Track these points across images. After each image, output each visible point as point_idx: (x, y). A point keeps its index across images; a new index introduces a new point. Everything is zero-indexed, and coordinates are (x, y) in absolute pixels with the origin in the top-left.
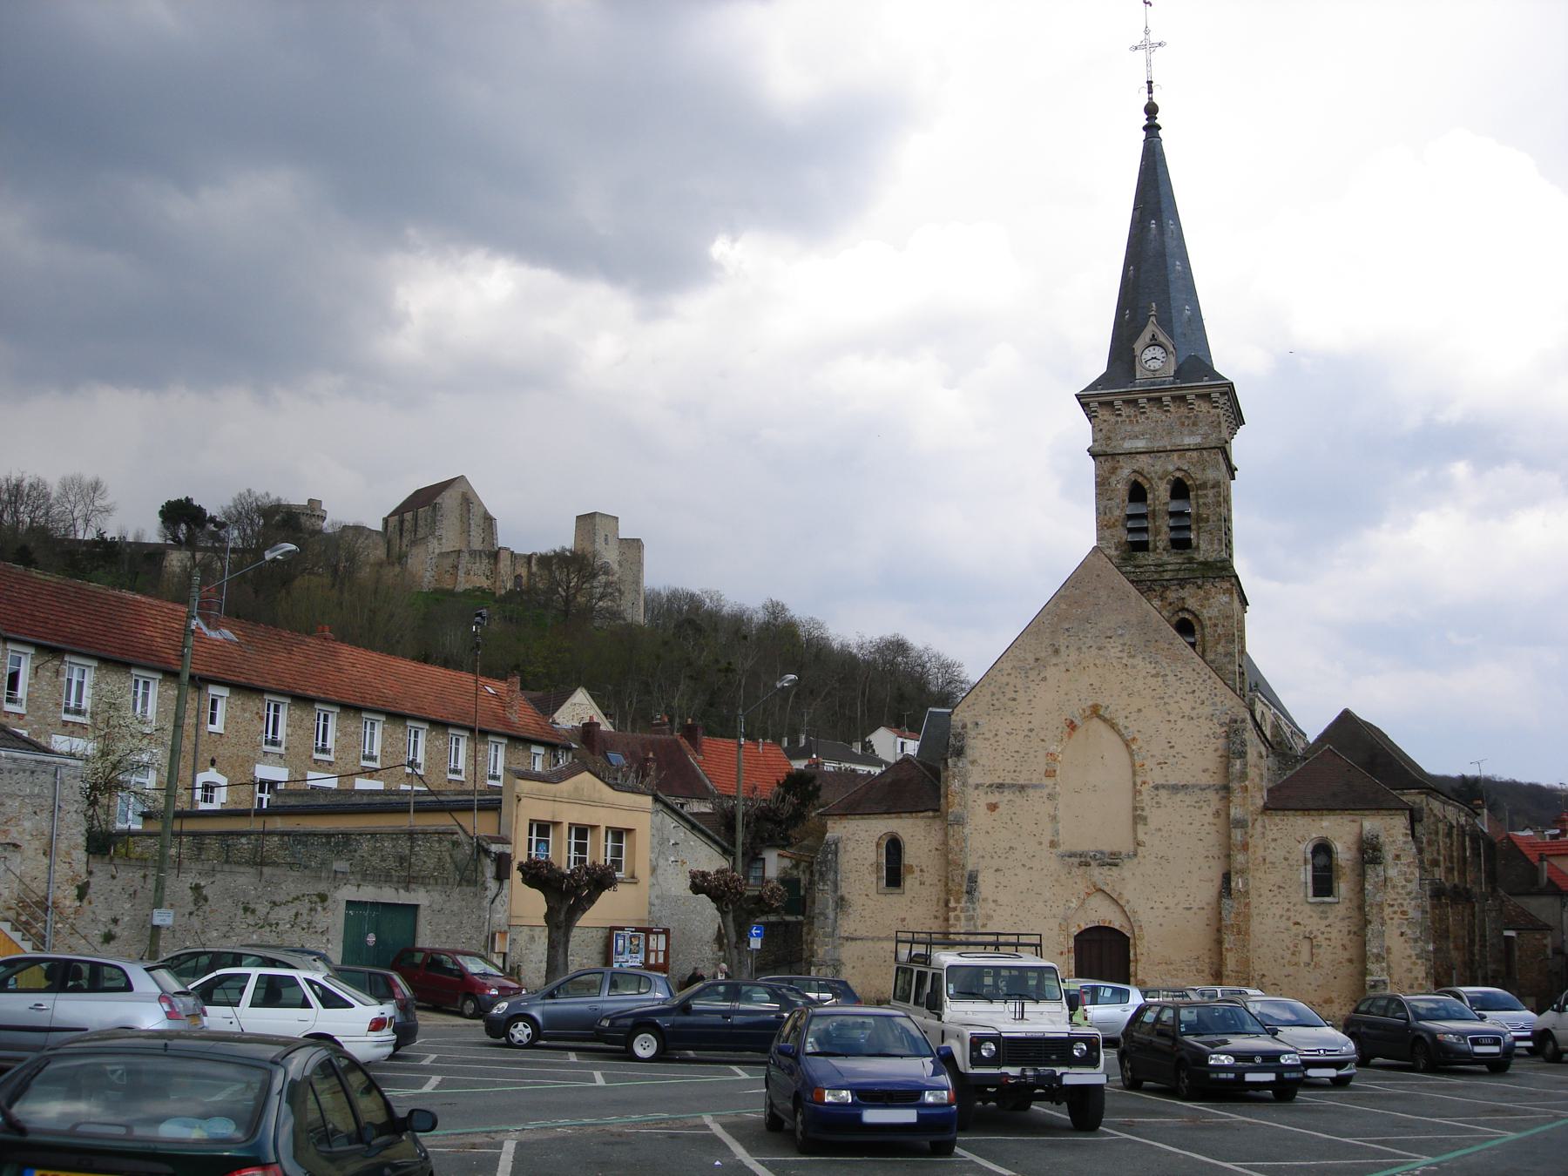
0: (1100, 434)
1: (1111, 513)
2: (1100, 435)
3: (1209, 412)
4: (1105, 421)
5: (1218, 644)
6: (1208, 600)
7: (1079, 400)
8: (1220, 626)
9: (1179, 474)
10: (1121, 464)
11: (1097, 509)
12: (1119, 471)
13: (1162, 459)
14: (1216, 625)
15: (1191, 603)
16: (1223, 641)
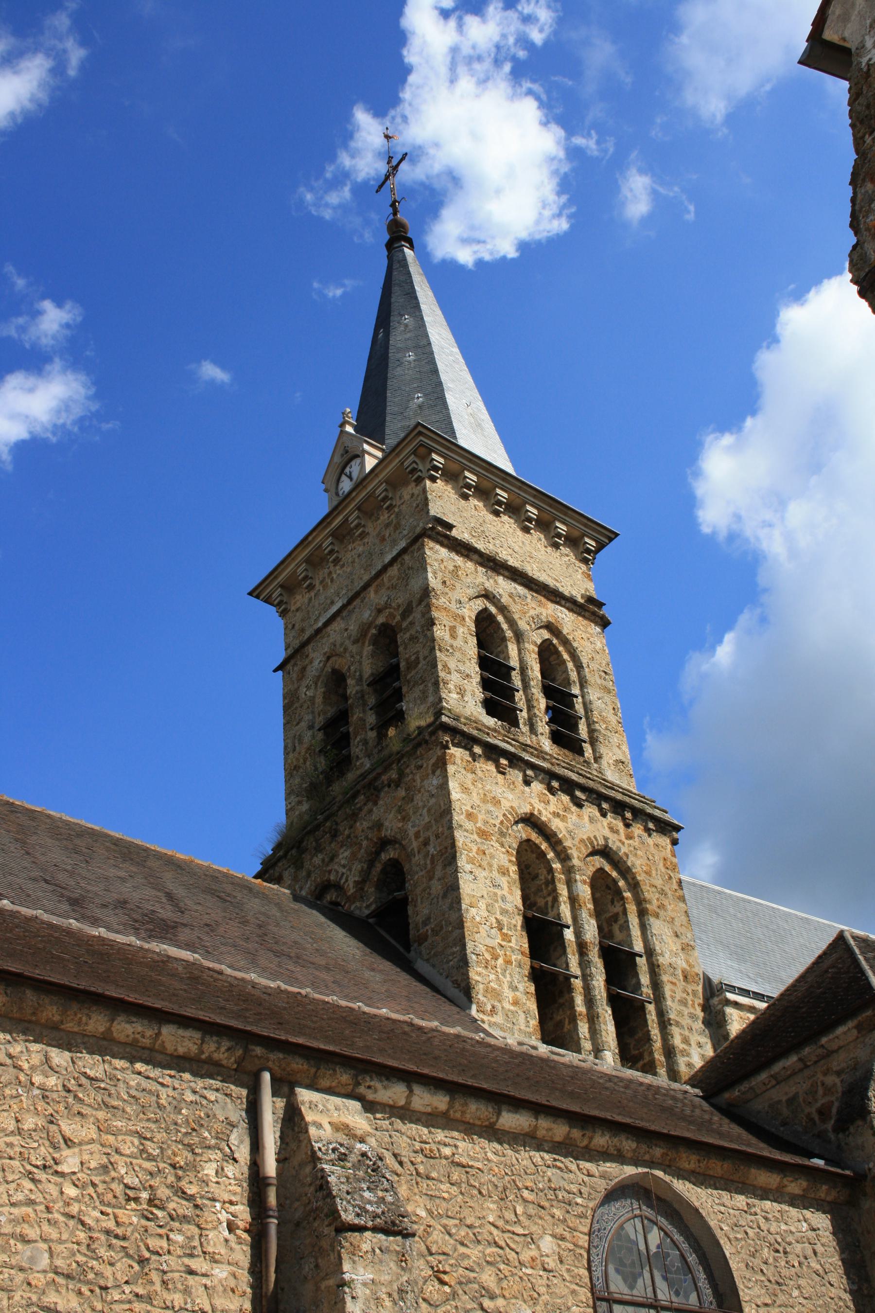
0: (293, 633)
1: (301, 742)
2: (293, 633)
3: (413, 495)
4: (297, 610)
5: (431, 878)
6: (412, 800)
7: (257, 597)
8: (432, 838)
9: (381, 620)
10: (311, 655)
11: (286, 747)
12: (309, 668)
13: (357, 610)
14: (426, 843)
15: (391, 825)
16: (439, 868)
